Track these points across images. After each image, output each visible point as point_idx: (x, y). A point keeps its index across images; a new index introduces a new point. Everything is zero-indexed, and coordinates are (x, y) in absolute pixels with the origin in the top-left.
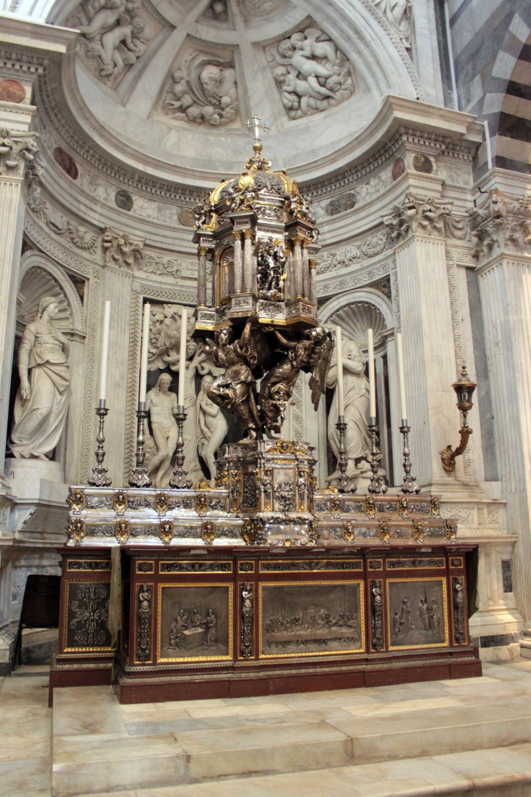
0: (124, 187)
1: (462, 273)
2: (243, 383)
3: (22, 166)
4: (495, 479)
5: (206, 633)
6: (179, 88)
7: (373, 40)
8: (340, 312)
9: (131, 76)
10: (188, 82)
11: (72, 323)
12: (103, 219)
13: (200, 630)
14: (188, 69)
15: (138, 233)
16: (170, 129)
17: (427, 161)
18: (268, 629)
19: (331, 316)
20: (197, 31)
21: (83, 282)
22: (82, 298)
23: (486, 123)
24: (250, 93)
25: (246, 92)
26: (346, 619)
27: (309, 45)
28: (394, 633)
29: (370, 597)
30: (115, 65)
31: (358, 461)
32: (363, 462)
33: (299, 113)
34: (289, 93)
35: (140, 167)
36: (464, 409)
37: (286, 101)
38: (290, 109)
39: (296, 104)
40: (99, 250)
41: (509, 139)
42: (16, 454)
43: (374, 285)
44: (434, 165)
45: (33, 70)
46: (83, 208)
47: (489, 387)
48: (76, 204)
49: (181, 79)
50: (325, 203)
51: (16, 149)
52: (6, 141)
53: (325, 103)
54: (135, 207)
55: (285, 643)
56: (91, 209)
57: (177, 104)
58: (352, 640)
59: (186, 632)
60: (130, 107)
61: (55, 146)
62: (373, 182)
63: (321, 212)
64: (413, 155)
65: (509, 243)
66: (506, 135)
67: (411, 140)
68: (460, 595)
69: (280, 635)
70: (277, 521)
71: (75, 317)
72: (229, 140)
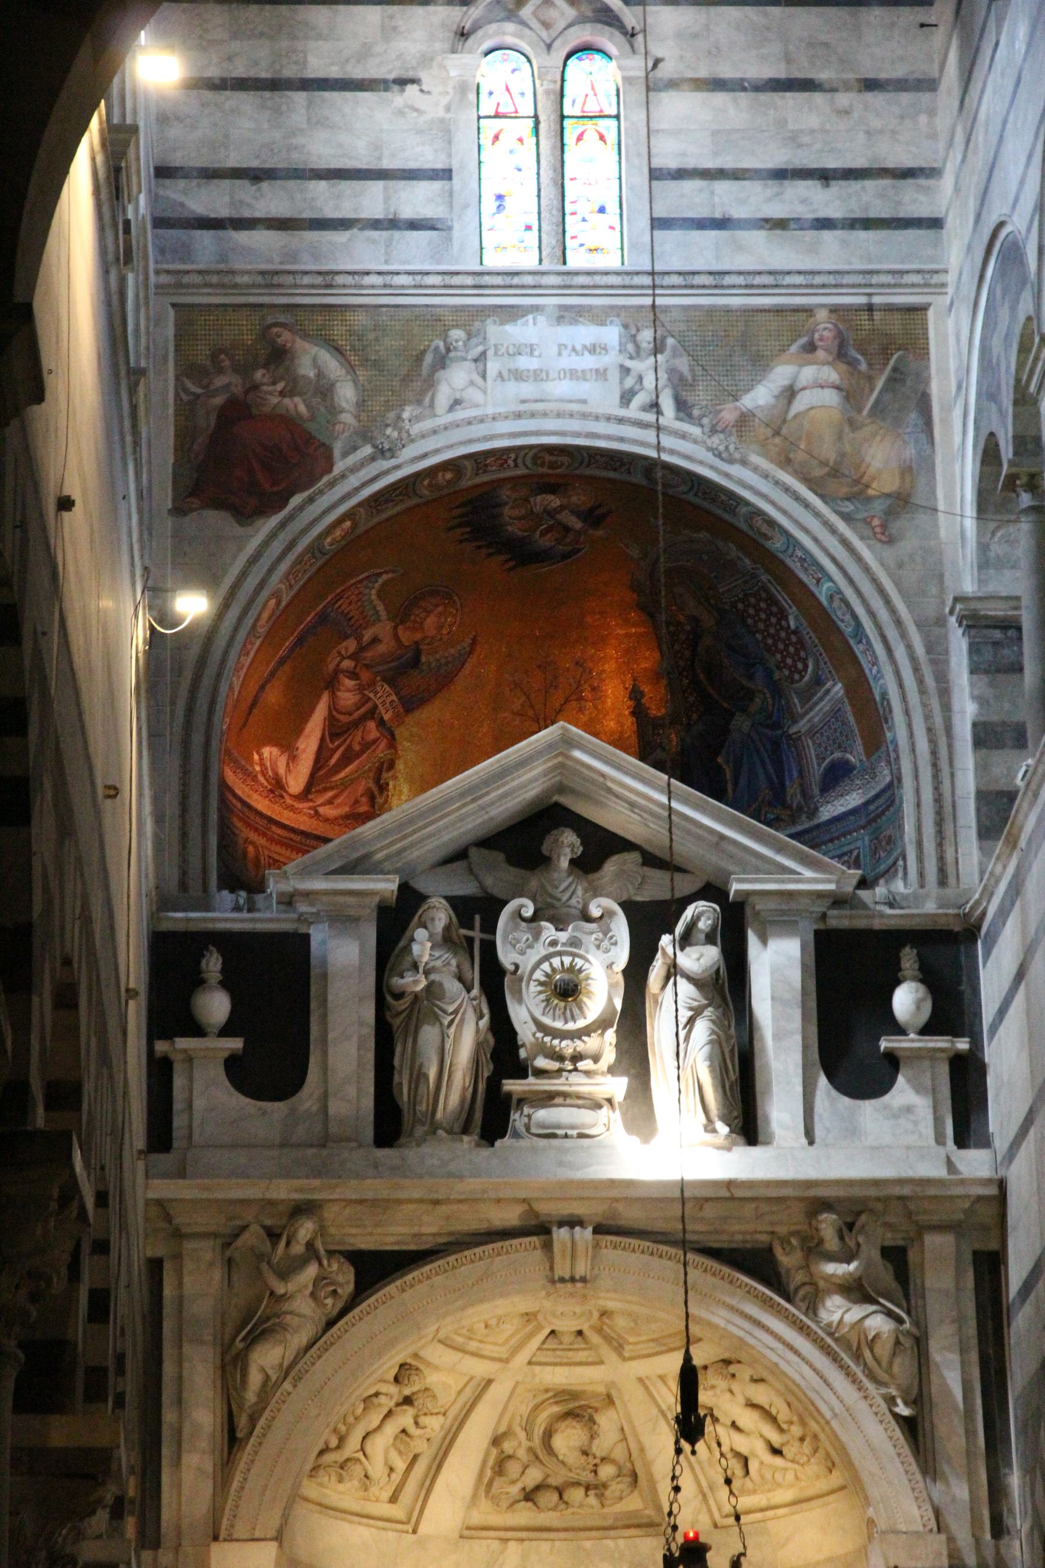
6: (513, 1469)
7: (836, 1415)
10: (531, 1450)
14: (528, 1429)
20: (534, 1375)
25: (642, 1450)
30: (392, 1469)
39: (739, 1471)
57: (515, 1490)
72: (621, 1542)
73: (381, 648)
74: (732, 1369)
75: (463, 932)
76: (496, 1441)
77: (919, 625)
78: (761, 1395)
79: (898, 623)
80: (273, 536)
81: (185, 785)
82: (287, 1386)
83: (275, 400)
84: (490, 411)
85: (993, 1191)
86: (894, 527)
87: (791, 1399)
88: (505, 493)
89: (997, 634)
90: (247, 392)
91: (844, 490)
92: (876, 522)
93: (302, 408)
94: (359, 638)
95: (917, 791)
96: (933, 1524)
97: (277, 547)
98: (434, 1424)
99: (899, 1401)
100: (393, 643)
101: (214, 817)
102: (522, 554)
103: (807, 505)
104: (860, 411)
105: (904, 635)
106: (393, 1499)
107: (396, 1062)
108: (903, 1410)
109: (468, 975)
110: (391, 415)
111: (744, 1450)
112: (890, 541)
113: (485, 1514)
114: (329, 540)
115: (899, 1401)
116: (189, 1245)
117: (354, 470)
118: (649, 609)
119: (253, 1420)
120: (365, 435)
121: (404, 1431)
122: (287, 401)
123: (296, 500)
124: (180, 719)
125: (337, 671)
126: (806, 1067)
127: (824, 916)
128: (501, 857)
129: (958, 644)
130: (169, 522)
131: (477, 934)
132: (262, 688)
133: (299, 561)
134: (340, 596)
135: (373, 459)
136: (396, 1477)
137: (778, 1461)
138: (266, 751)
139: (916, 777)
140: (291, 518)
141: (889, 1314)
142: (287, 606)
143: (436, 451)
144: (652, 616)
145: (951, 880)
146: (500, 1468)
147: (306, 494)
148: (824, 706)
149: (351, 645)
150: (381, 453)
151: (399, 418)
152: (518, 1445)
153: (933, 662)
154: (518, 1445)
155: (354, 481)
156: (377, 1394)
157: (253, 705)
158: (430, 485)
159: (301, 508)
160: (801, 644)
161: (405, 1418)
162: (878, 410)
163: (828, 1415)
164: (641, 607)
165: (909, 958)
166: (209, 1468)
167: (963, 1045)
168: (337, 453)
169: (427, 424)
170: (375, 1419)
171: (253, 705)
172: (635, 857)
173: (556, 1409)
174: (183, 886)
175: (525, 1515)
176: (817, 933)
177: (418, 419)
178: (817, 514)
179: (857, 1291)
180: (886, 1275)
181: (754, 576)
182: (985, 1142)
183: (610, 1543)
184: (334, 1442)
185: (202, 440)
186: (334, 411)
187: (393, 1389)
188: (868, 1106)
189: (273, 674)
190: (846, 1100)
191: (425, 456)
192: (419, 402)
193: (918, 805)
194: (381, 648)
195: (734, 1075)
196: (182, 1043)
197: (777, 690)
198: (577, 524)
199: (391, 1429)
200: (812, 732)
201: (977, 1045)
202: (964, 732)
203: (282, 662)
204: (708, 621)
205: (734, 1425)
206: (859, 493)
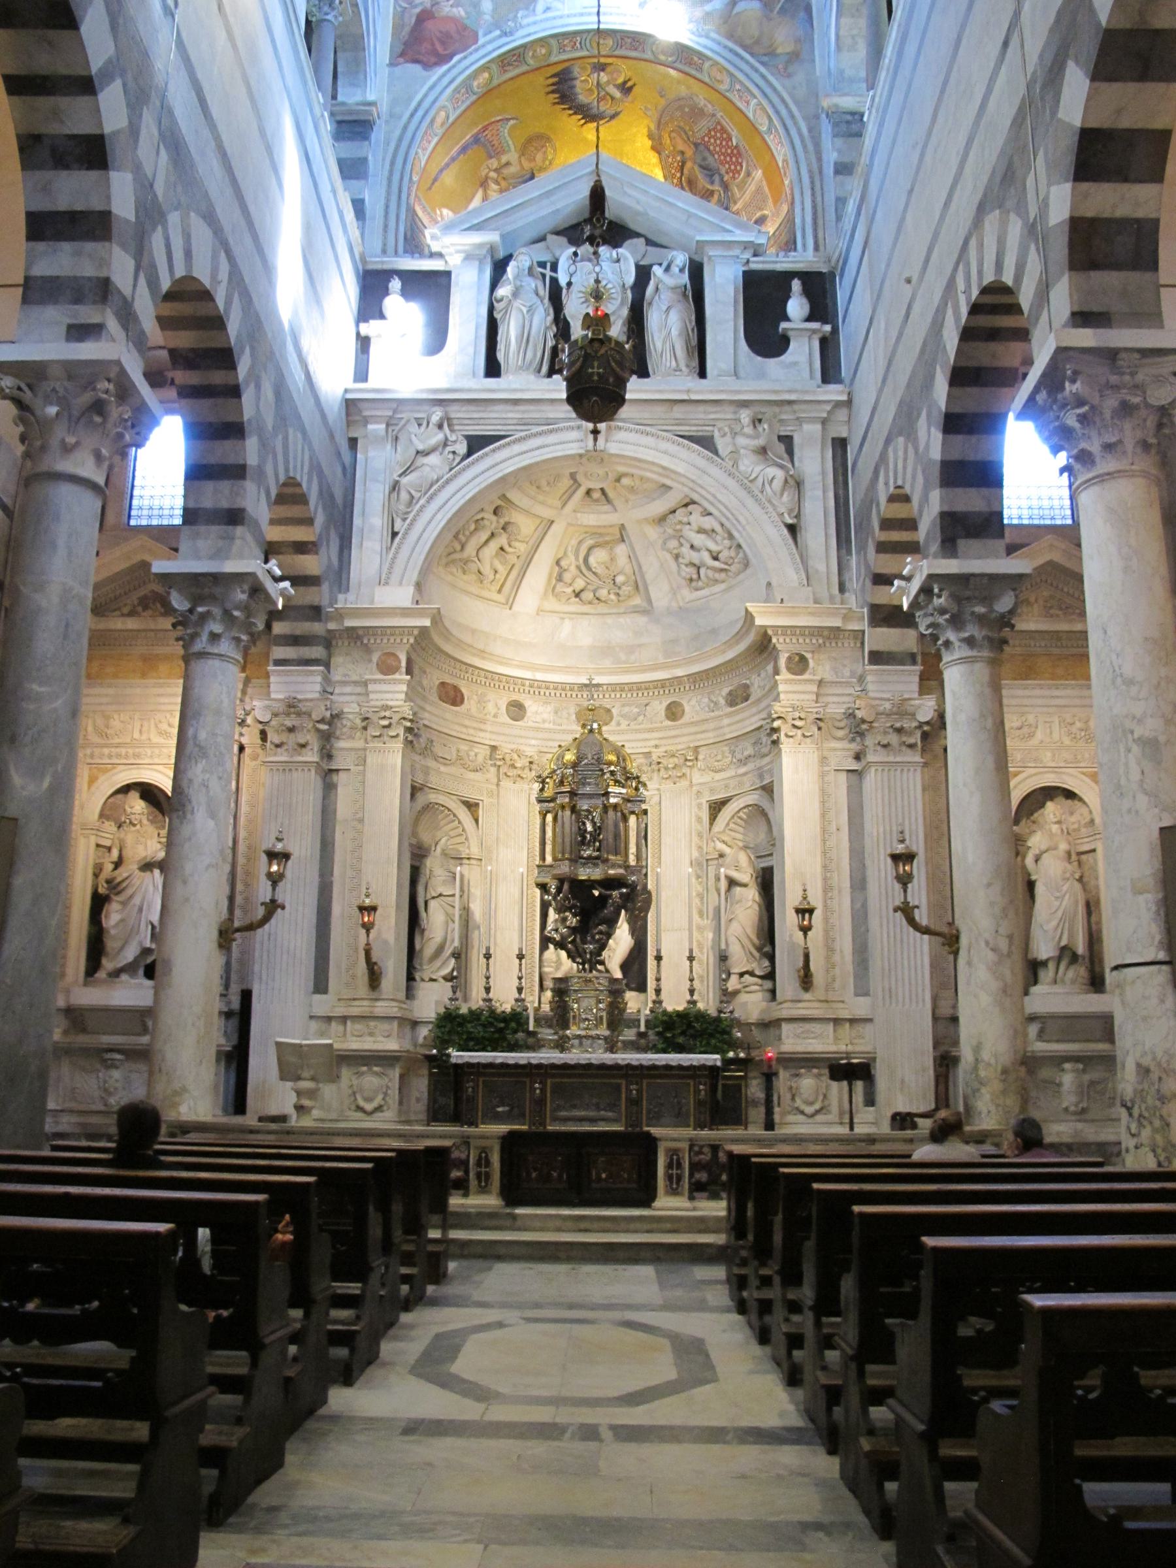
0: (515, 697)
1: (844, 776)
2: (568, 927)
3: (401, 731)
4: (867, 994)
5: (511, 1111)
6: (567, 577)
8: (741, 814)
9: (514, 573)
10: (578, 567)
11: (469, 848)
12: (494, 737)
13: (507, 1108)
15: (533, 742)
16: (563, 619)
17: (803, 659)
18: (554, 1110)
19: (733, 817)
21: (477, 805)
22: (477, 821)
23: (865, 610)
24: (644, 569)
25: (640, 567)
26: (613, 1106)
27: (697, 519)
28: (648, 1118)
29: (629, 1091)
31: (741, 975)
32: (747, 976)
33: (700, 583)
34: (686, 565)
35: (528, 675)
36: (805, 930)
37: (684, 574)
38: (691, 580)
39: (695, 576)
40: (493, 770)
41: (885, 630)
42: (417, 978)
43: (764, 788)
44: (811, 661)
45: (405, 641)
46: (472, 731)
47: (866, 900)
48: (464, 730)
49: (570, 565)
50: (725, 691)
51: (396, 717)
52: (387, 714)
53: (723, 575)
54: (528, 714)
55: (566, 1120)
56: (481, 730)
57: (569, 590)
58: (615, 1121)
59: (500, 1109)
60: (515, 608)
61: (437, 683)
62: (763, 674)
63: (722, 701)
64: (787, 655)
65: (879, 748)
66: (880, 626)
67: (781, 640)
68: (703, 1093)
69: (563, 1114)
70: (579, 1037)
71: (471, 841)
73: (512, 170)
74: (690, 507)
75: (540, 270)
76: (558, 563)
77: (805, 118)
78: (708, 522)
79: (792, 117)
80: (444, 75)
81: (388, 200)
82: (422, 502)
83: (447, 9)
84: (566, 12)
85: (844, 398)
86: (791, 69)
87: (724, 520)
88: (576, 71)
89: (849, 118)
90: (433, 6)
91: (762, 51)
92: (780, 66)
93: (463, 13)
94: (499, 160)
95: (803, 203)
96: (805, 582)
97: (446, 80)
98: (521, 548)
99: (786, 515)
100: (518, 168)
101: (403, 216)
102: (589, 115)
103: (742, 58)
104: (772, 11)
105: (796, 124)
106: (499, 591)
107: (499, 338)
108: (790, 521)
109: (541, 292)
110: (511, 16)
111: (697, 562)
112: (789, 76)
113: (552, 604)
114: (475, 84)
115: (786, 515)
116: (370, 427)
117: (490, 42)
118: (657, 148)
119: (404, 520)
120: (496, 25)
121: (502, 549)
122: (454, 10)
123: (456, 59)
124: (387, 167)
125: (487, 178)
126: (736, 340)
127: (748, 262)
128: (563, 240)
129: (826, 128)
130: (387, 70)
131: (548, 273)
132: (441, 171)
133: (457, 91)
134: (485, 128)
135: (500, 37)
136: (500, 577)
137: (716, 564)
138: (445, 211)
139: (802, 194)
140: (454, 66)
141: (782, 467)
142: (453, 124)
143: (535, 33)
144: (659, 153)
145: (822, 248)
146: (560, 579)
147: (461, 55)
148: (752, 188)
149: (494, 163)
150: (505, 34)
151: (516, 16)
152: (570, 562)
153: (812, 137)
154: (570, 562)
155: (490, 48)
156: (483, 519)
157: (435, 180)
158: (533, 56)
159: (460, 61)
160: (740, 154)
161: (502, 540)
162: (783, 11)
163: (744, 522)
164: (653, 148)
165: (796, 285)
166: (378, 547)
167: (828, 328)
168: (480, 33)
169: (531, 20)
170: (484, 536)
171: (435, 180)
172: (642, 240)
173: (590, 542)
174: (384, 252)
175: (575, 606)
176: (744, 272)
177: (526, 16)
178: (747, 62)
179: (763, 451)
180: (781, 448)
181: (714, 115)
182: (839, 381)
183: (621, 620)
184: (458, 547)
185: (407, 29)
186: (480, 13)
187: (494, 518)
188: (772, 363)
189: (447, 165)
190: (759, 358)
191: (529, 35)
192: (527, 9)
193: (803, 209)
194: (512, 170)
195: (694, 342)
196: (374, 324)
197: (726, 187)
198: (617, 94)
199: (494, 546)
200: (746, 206)
201: (835, 331)
202: (829, 170)
203: (453, 159)
204: (689, 153)
205: (692, 547)
206: (772, 54)
